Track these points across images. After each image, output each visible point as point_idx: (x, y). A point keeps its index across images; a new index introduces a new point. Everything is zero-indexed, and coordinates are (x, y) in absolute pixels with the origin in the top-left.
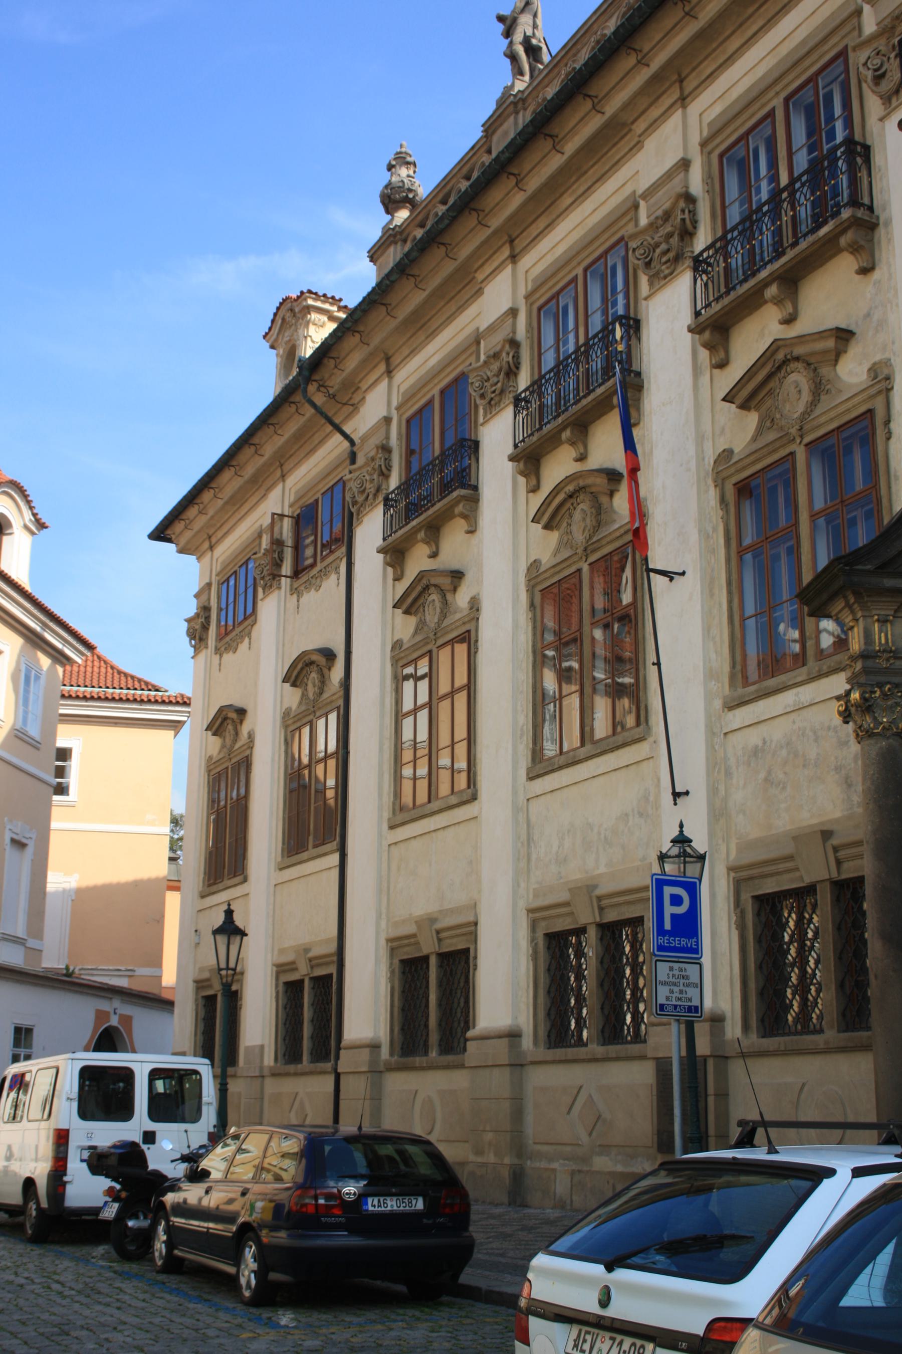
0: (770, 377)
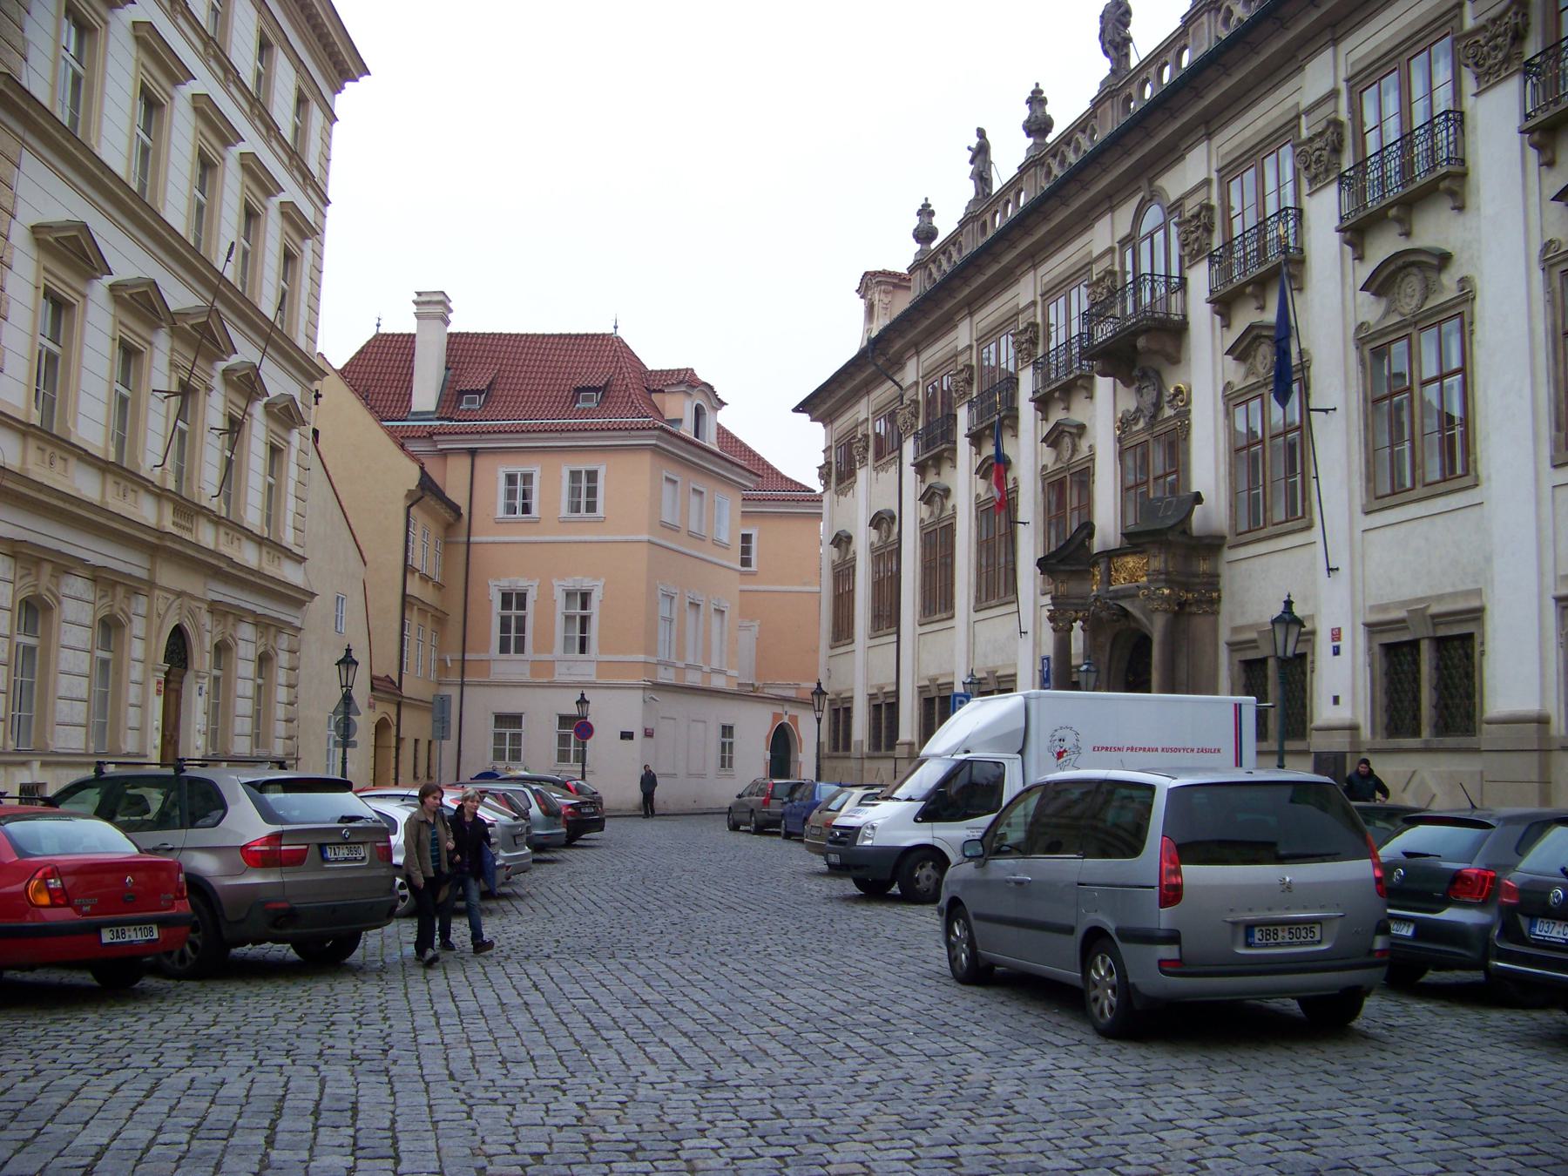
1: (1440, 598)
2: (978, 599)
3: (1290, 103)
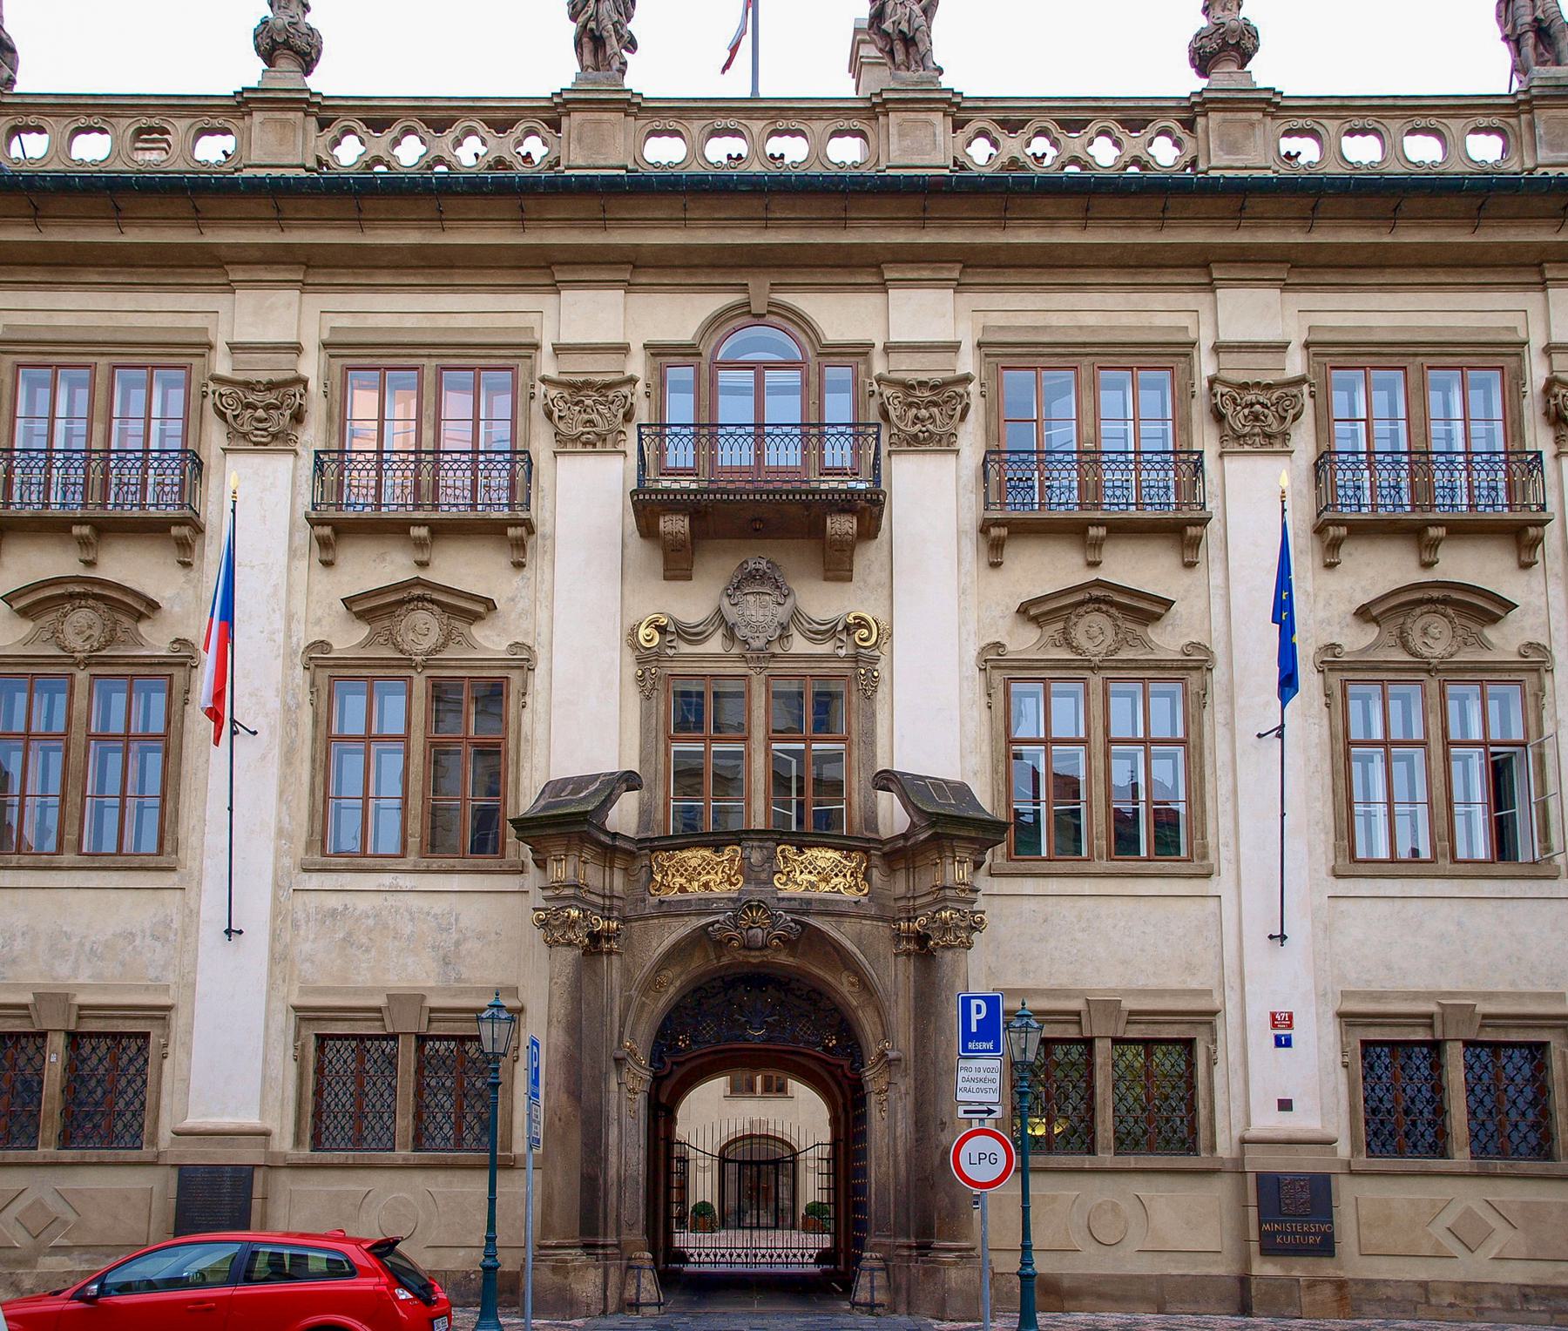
0: (401, 603)
1: (1489, 996)
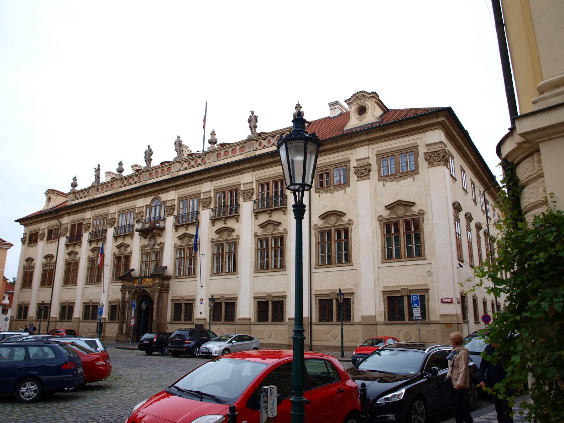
1: (227, 295)
2: (86, 282)
3: (198, 189)
